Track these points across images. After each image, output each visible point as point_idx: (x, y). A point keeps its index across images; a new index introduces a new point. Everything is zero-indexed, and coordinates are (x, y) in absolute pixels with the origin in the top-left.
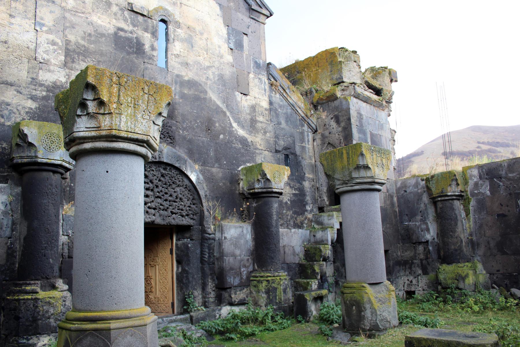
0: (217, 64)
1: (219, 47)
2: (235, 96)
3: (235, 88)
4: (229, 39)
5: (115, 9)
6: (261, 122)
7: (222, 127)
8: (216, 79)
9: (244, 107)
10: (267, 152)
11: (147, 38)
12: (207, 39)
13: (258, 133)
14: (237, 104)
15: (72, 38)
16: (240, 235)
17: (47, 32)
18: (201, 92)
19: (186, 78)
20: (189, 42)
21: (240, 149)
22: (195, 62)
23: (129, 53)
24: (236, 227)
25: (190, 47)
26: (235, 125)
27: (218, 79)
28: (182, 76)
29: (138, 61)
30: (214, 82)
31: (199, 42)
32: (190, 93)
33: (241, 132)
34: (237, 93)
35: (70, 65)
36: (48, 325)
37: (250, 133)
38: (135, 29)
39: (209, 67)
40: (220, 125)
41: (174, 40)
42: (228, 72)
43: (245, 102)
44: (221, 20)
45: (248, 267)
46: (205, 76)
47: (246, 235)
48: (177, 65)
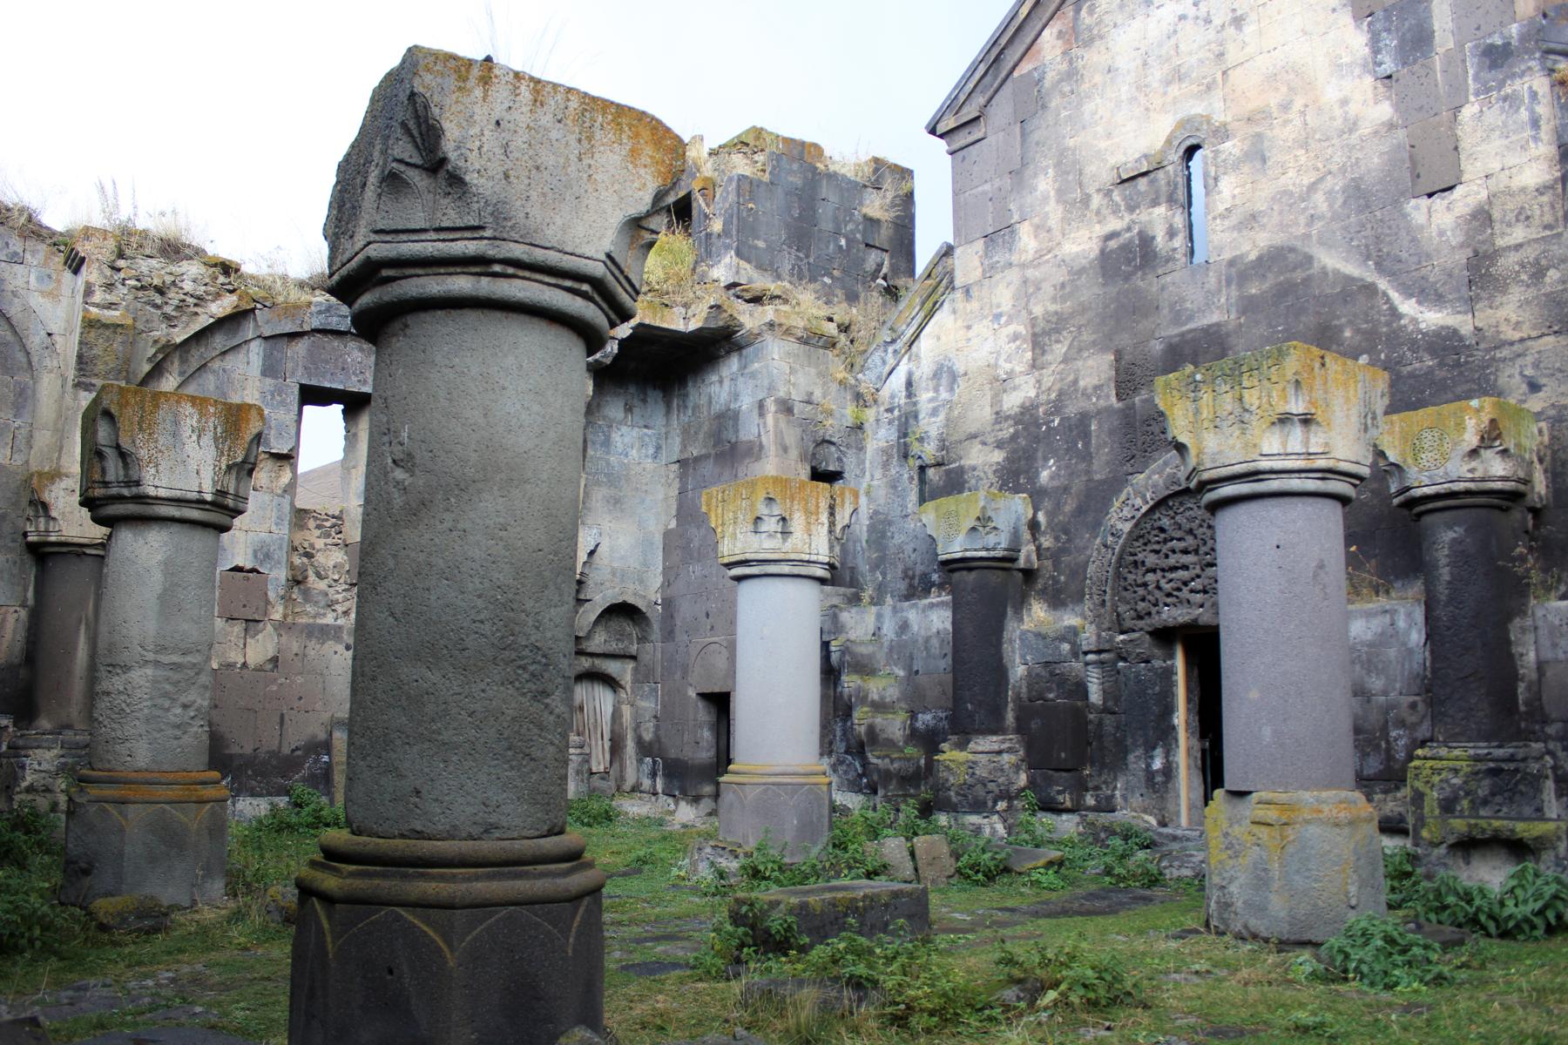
0: (1339, 158)
1: (1344, 102)
2: (1405, 216)
3: (1403, 194)
4: (1376, 51)
5: (1097, 200)
6: (1518, 247)
7: (1364, 332)
8: (1340, 202)
9: (1441, 233)
10: (1551, 339)
11: (1158, 219)
12: (1303, 113)
13: (1504, 290)
14: (1414, 240)
15: (1038, 310)
16: (1382, 634)
17: (1008, 323)
18: (1294, 269)
19: (1253, 256)
20: (1257, 155)
21: (1431, 370)
22: (1273, 199)
23: (1127, 277)
24: (1369, 615)
25: (1258, 165)
26: (1408, 307)
27: (1345, 202)
28: (1241, 257)
29: (1146, 283)
30: (1332, 219)
31: (1283, 134)
32: (1266, 286)
33: (1431, 318)
34: (1413, 202)
35: (1038, 363)
36: (948, 799)
37: (1471, 304)
38: (1134, 216)
39: (1312, 187)
40: (1358, 331)
41: (1216, 179)
42: (1373, 160)
43: (1439, 221)
44: (1346, 18)
45: (1413, 727)
46: (1302, 220)
47: (1407, 632)
48: (1227, 237)
